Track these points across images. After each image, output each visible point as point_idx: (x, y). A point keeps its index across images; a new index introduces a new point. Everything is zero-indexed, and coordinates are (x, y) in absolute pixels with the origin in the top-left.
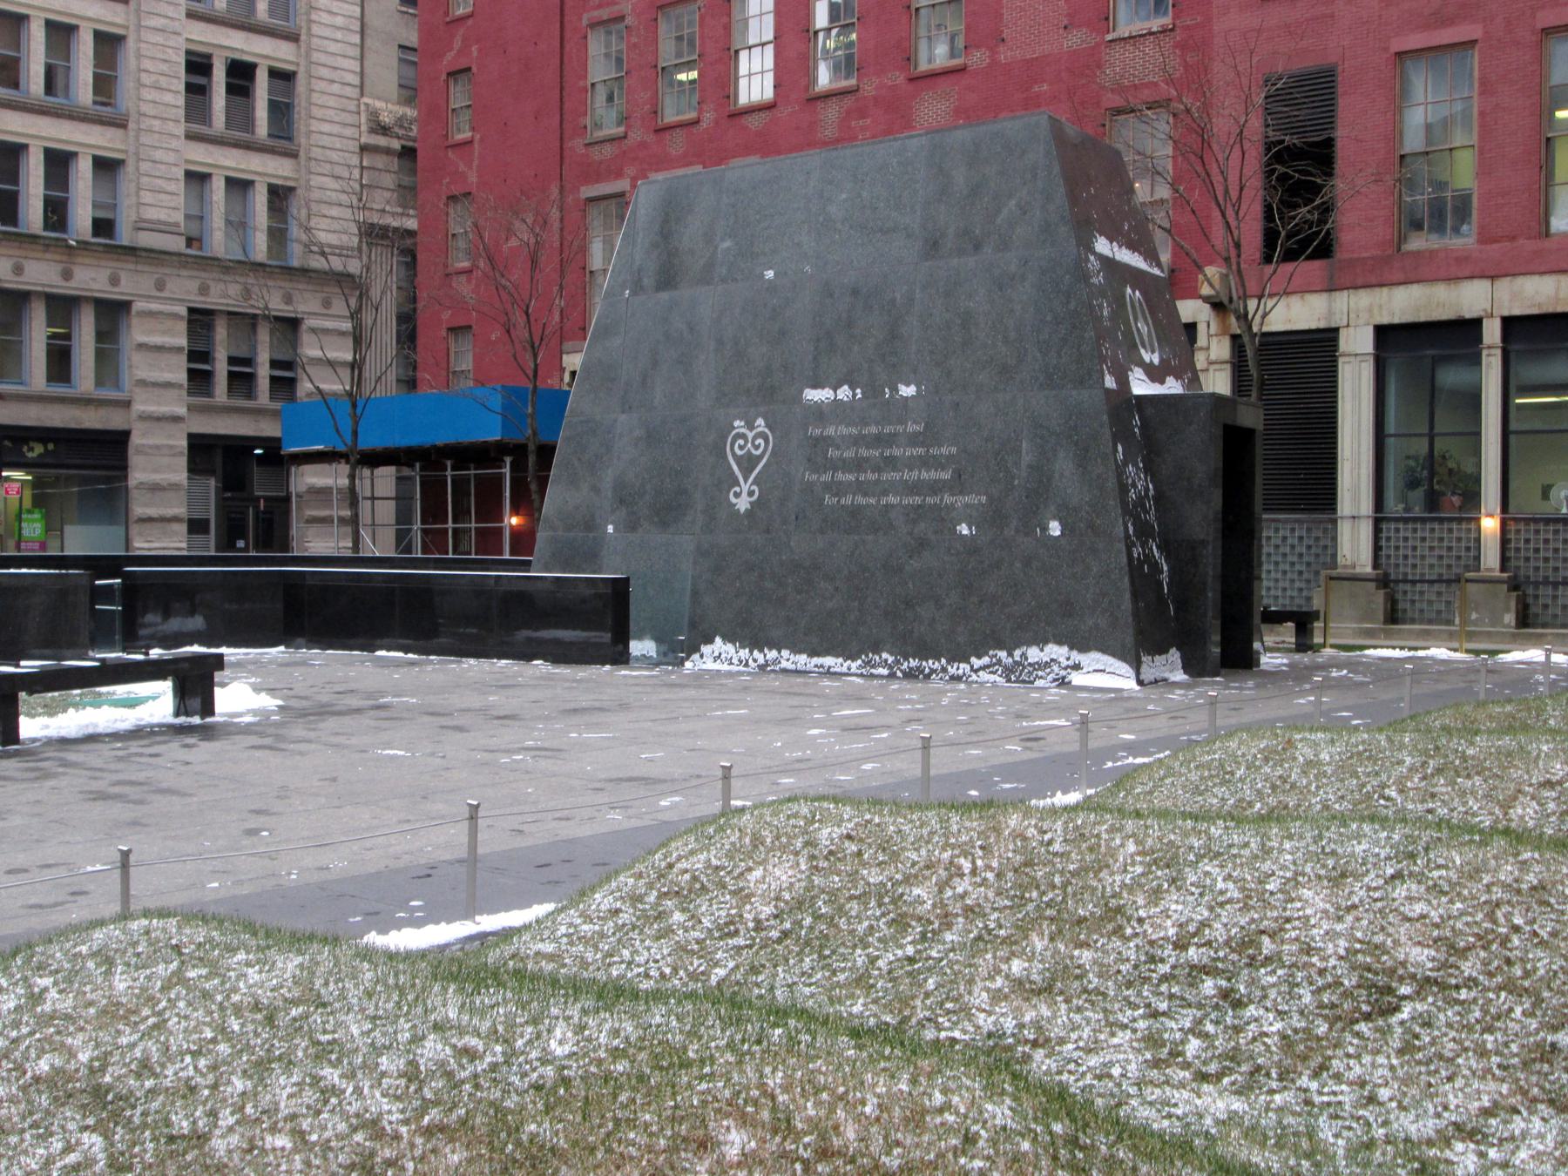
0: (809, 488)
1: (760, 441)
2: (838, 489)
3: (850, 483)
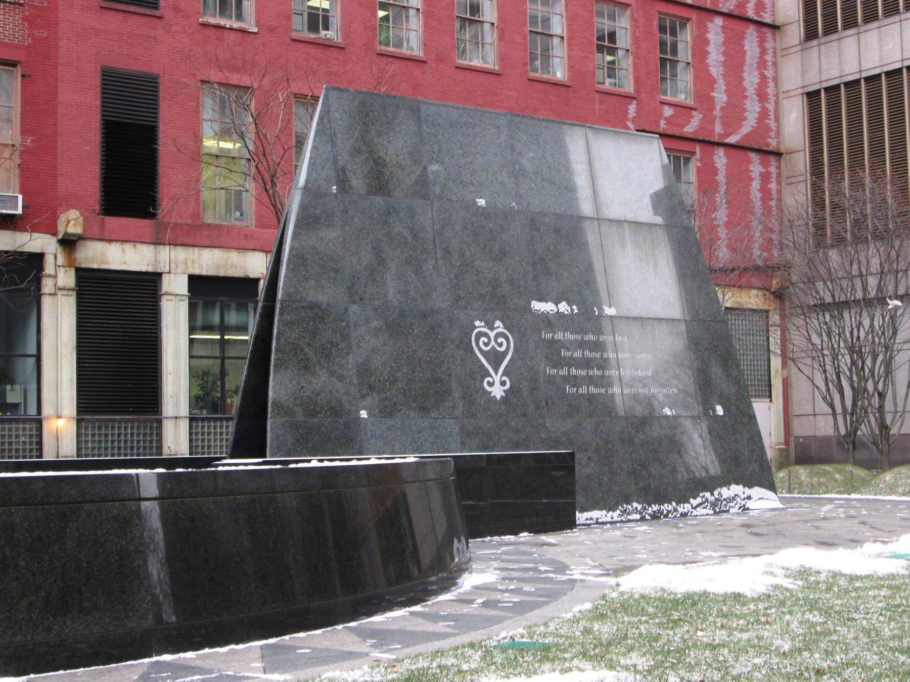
0: (551, 380)
1: (500, 340)
2: (575, 381)
3: (583, 377)
